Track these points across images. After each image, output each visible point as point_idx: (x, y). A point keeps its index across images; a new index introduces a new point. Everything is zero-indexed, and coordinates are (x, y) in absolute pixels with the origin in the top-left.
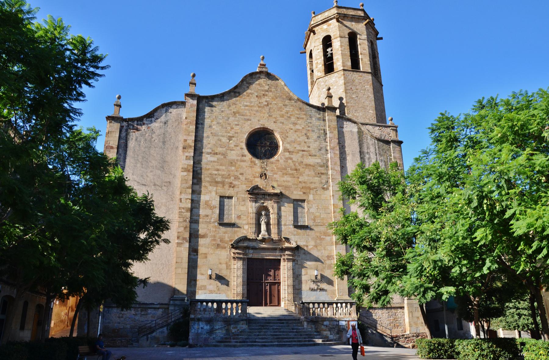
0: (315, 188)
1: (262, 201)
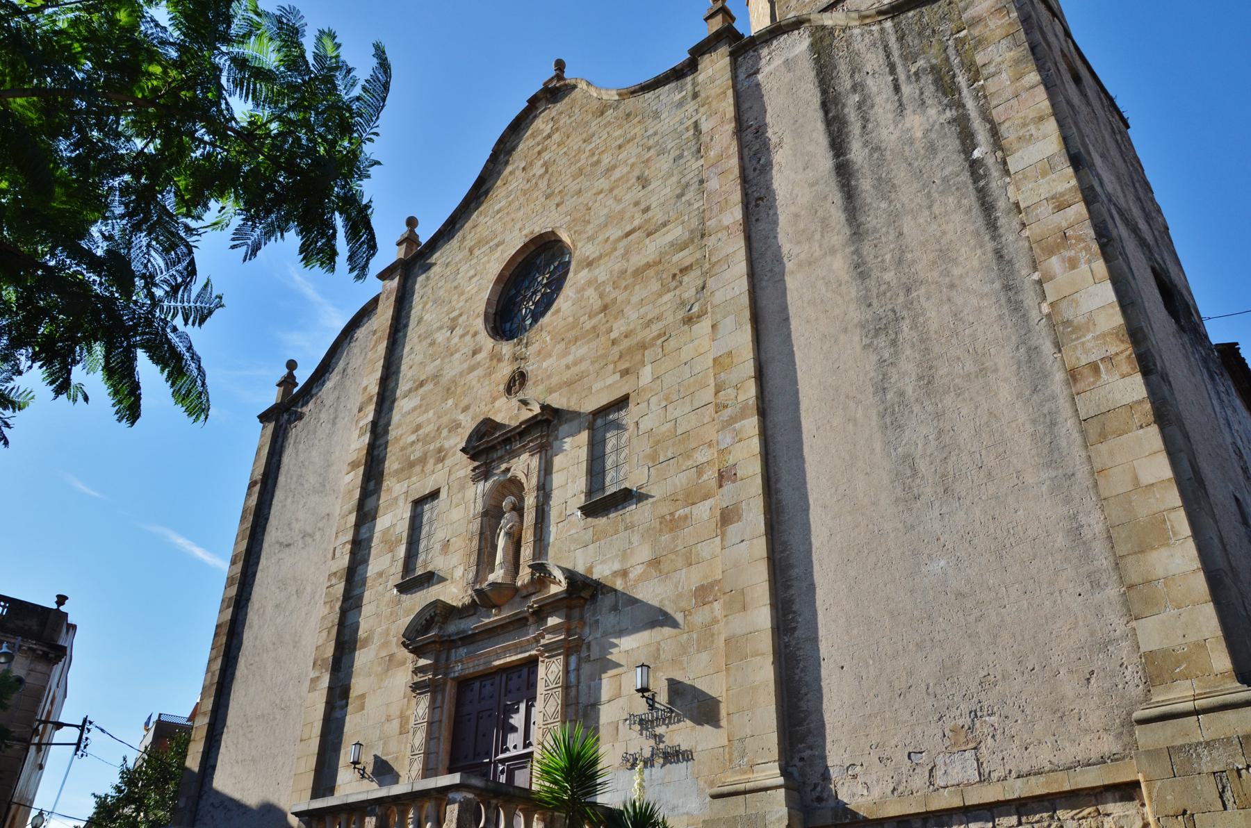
0: (659, 336)
1: (504, 466)
